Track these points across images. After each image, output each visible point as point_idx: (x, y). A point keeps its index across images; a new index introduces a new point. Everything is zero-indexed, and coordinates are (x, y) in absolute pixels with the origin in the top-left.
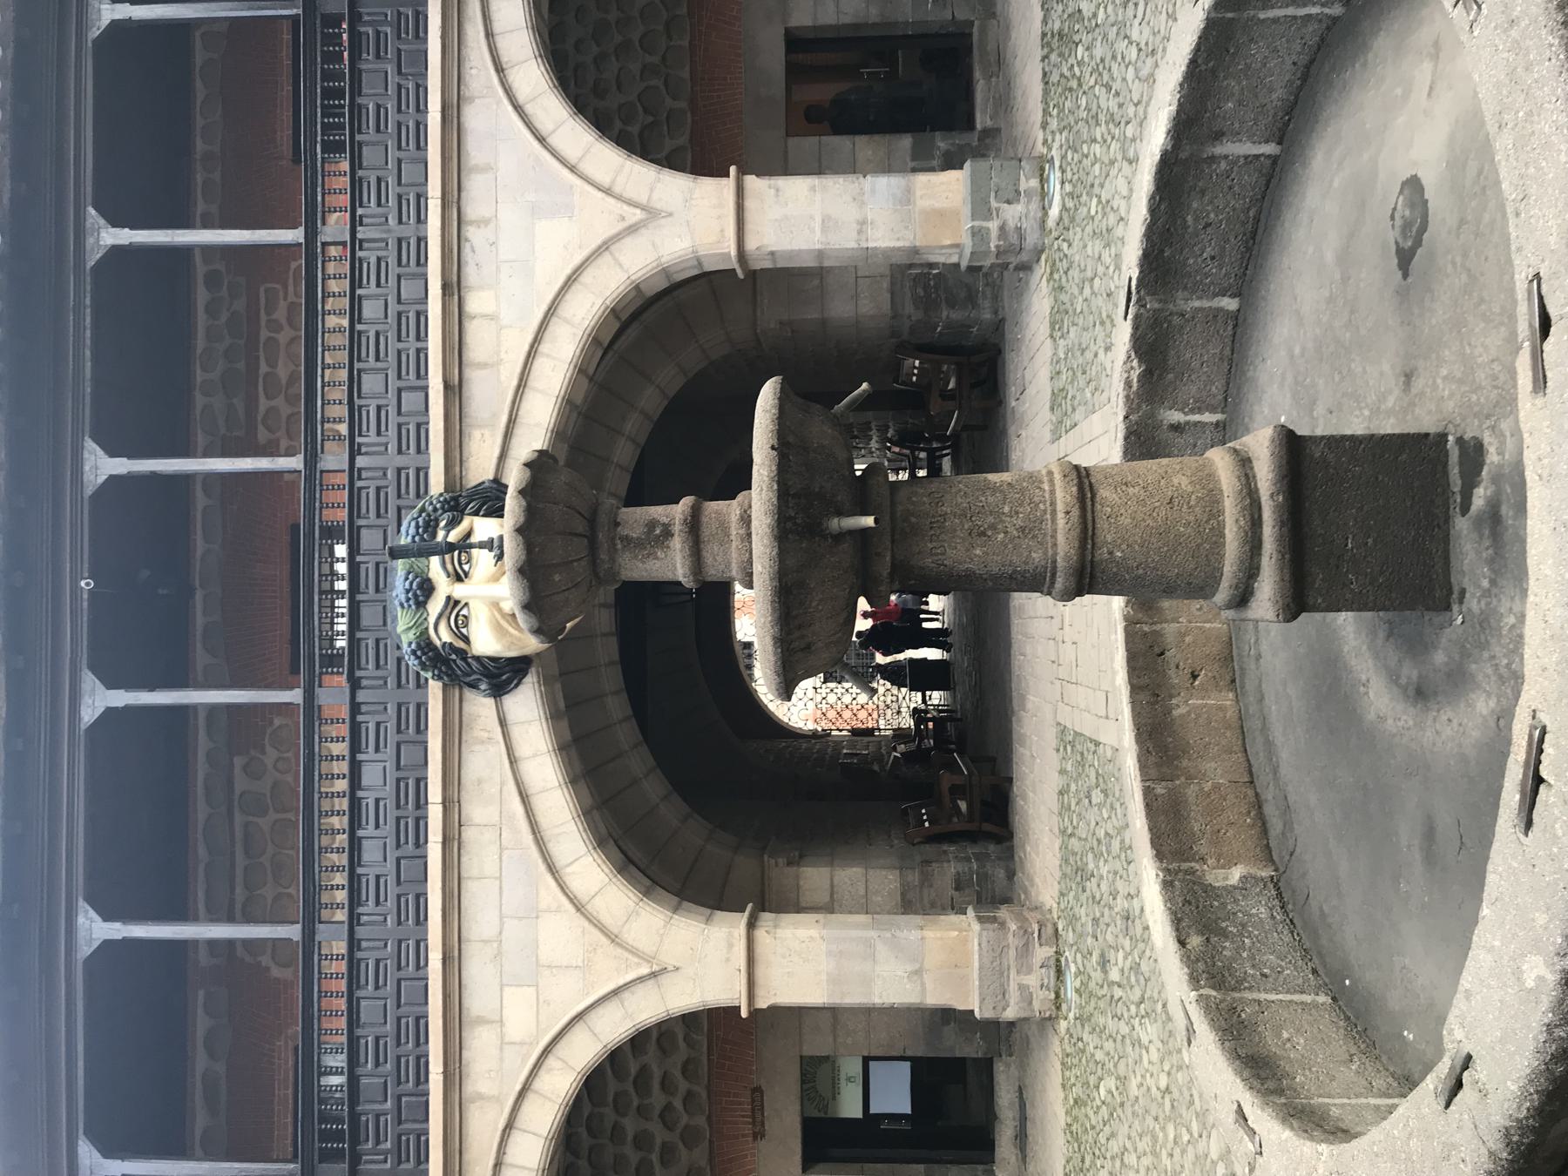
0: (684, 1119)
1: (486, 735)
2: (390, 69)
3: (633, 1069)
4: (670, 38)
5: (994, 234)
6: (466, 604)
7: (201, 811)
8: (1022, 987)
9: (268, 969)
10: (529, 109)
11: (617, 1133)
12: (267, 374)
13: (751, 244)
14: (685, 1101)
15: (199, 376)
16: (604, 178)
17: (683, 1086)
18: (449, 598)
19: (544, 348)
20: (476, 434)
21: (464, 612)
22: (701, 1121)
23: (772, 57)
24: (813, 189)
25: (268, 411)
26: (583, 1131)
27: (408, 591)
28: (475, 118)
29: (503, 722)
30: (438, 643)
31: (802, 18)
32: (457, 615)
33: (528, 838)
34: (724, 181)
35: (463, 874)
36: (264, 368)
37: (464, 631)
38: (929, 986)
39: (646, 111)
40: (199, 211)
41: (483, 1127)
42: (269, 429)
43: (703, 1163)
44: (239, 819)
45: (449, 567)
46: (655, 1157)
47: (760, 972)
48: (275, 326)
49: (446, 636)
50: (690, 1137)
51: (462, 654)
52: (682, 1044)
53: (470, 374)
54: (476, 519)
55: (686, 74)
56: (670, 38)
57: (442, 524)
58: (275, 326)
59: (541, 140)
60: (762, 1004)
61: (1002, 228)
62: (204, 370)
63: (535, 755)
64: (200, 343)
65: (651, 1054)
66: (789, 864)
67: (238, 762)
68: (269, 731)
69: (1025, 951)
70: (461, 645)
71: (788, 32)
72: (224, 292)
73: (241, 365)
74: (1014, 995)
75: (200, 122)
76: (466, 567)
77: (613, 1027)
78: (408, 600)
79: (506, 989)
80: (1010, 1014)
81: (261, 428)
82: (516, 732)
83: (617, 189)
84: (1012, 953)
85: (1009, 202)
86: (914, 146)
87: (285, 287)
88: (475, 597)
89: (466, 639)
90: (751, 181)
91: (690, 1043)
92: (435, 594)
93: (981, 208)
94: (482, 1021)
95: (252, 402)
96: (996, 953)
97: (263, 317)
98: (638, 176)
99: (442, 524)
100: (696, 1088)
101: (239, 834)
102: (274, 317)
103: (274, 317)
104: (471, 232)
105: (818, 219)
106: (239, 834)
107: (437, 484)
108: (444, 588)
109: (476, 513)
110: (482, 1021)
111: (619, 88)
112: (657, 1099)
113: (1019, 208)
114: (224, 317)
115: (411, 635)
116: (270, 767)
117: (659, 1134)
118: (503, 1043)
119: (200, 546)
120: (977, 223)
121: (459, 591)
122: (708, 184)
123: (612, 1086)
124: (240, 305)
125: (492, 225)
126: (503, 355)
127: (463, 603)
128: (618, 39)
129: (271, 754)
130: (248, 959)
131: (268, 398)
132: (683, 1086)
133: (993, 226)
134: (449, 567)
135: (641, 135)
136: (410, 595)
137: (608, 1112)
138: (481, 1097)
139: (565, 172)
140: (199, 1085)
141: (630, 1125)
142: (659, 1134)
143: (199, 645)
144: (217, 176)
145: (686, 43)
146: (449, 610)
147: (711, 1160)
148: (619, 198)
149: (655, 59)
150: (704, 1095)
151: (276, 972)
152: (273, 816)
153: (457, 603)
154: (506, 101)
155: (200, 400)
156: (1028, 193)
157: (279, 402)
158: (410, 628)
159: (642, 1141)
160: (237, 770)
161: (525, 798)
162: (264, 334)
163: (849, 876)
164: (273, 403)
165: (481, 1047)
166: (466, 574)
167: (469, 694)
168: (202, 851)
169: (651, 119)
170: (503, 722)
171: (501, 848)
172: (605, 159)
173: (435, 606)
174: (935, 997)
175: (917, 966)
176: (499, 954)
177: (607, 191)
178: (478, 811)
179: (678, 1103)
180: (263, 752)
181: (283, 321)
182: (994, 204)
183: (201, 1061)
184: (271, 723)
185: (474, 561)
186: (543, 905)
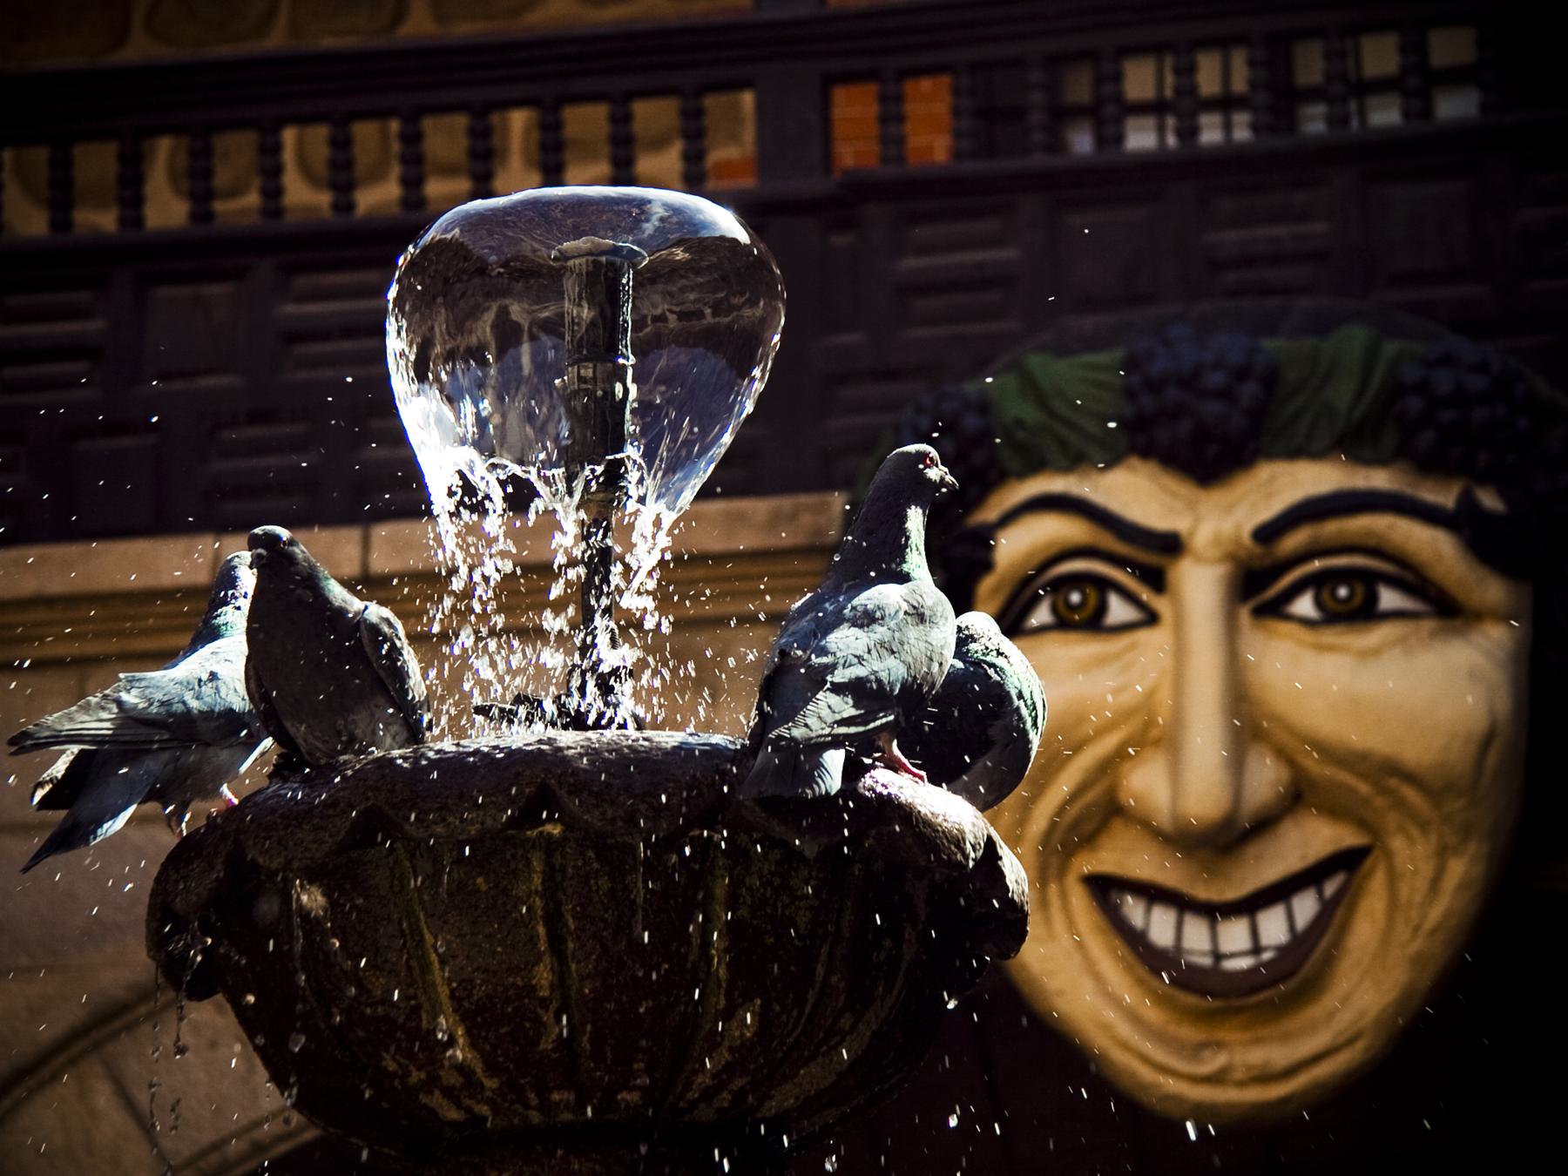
6: (1151, 618)
18: (1172, 545)
21: (1118, 610)
27: (1189, 381)
30: (990, 512)
32: (1104, 585)
45: (1294, 541)
57: (1489, 500)
76: (1304, 606)
78: (1154, 387)
88: (1180, 651)
92: (1183, 489)
99: (1489, 500)
115: (1019, 409)
127: (1161, 604)
134: (1294, 541)
136: (1173, 393)
146: (1122, 548)
153: (1156, 580)
158: (1041, 401)
166: (1274, 610)
185: (1330, 636)
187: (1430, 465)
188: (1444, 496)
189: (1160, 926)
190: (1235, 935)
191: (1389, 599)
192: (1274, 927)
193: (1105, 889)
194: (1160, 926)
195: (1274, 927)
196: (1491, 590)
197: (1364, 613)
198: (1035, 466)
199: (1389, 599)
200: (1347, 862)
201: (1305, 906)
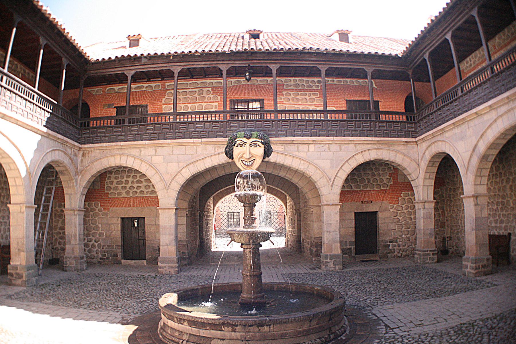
0: (131, 191)
1: (216, 150)
2: (361, 128)
3: (142, 180)
4: (376, 185)
5: (327, 261)
7: (199, 81)
8: (165, 267)
9: (164, 98)
10: (353, 158)
11: (128, 176)
12: (298, 93)
13: (325, 207)
14: (135, 191)
15: (297, 79)
16: (339, 175)
17: (138, 191)
19: (302, 161)
20: (283, 147)
21: (243, 146)
22: (131, 195)
23: (371, 208)
24: (337, 221)
25: (290, 94)
26: (128, 169)
28: (352, 146)
29: (219, 154)
30: (236, 140)
31: (380, 215)
33: (194, 160)
34: (339, 201)
35: (187, 147)
36: (300, 93)
37: (239, 146)
38: (164, 247)
39: (360, 180)
40: (334, 79)
41: (135, 152)
42: (286, 94)
43: (123, 196)
44: (197, 90)
46: (124, 185)
47: (167, 210)
48: (310, 95)
49: (238, 142)
50: (128, 193)
51: (234, 145)
52: (147, 190)
53: (296, 145)
54: (263, 148)
55: (368, 189)
56: (376, 185)
58: (310, 95)
59: (347, 161)
60: (160, 211)
61: (328, 262)
62: (299, 80)
63: (212, 161)
64: (305, 79)
65: (147, 187)
66: (187, 214)
67: (210, 89)
68: (217, 95)
69: (172, 267)
70: (236, 145)
71: (376, 213)
72: (317, 84)
73: (300, 88)
74: (163, 265)
75: (354, 80)
76: (253, 146)
77: (155, 180)
79: (162, 156)
80: (159, 264)
81: (286, 92)
82: (217, 156)
83: (337, 178)
84: (172, 265)
85: (333, 263)
86: (352, 241)
87: (318, 98)
89: (237, 146)
90: (339, 207)
91: (147, 192)
92: (247, 140)
93: (332, 257)
94: (156, 151)
95: (292, 90)
96: (172, 262)
97: (311, 93)
98: (340, 182)
99: (263, 141)
100: (138, 193)
101: (194, 90)
102: (312, 95)
103: (312, 95)
104: (327, 146)
105: (330, 222)
106: (194, 90)
107: (271, 139)
108: (249, 142)
109: (265, 147)
110: (156, 151)
111: (365, 173)
112: (135, 185)
113: (332, 265)
114: (311, 84)
116: (209, 96)
117: (128, 186)
118: (151, 156)
119: (259, 79)
120: (329, 257)
121: (247, 145)
122: (338, 198)
123: (138, 175)
124: (314, 88)
125: (328, 150)
126: (300, 153)
128: (376, 173)
129: (211, 96)
130: (167, 93)
131: (293, 94)
132: (138, 191)
133: (328, 260)
135: (355, 178)
137: (133, 174)
138: (141, 151)
139: (340, 167)
140: (140, 85)
141: (130, 179)
142: (128, 186)
143: (236, 79)
144: (342, 83)
145: (375, 189)
147: (123, 197)
148: (335, 178)
149: (371, 182)
150: (137, 196)
151: (164, 99)
152: (198, 97)
154: (355, 154)
155: (292, 79)
156: (335, 267)
157: (292, 96)
159: (127, 182)
160: (208, 89)
161: (202, 159)
162: (307, 93)
163: (183, 228)
164: (292, 95)
165: (151, 151)
167: (226, 146)
168: (191, 82)
169: (358, 180)
170: (219, 154)
171: (192, 154)
172: (343, 175)
173: (245, 140)
174: (161, 248)
175: (168, 244)
176: (170, 155)
177: (336, 176)
178: (200, 149)
179: (135, 190)
180: (212, 94)
181: (310, 97)
182: (333, 260)
183: (146, 85)
184: (219, 96)
186: (180, 164)
187: (260, 139)
188: (260, 141)
189: (245, 162)
190: (248, 163)
191: (257, 146)
192: (251, 163)
193: (242, 160)
194: (245, 162)
195: (251, 163)
196: (263, 146)
197: (256, 147)
198: (239, 138)
199: (257, 146)
200: (255, 159)
201: (252, 162)
